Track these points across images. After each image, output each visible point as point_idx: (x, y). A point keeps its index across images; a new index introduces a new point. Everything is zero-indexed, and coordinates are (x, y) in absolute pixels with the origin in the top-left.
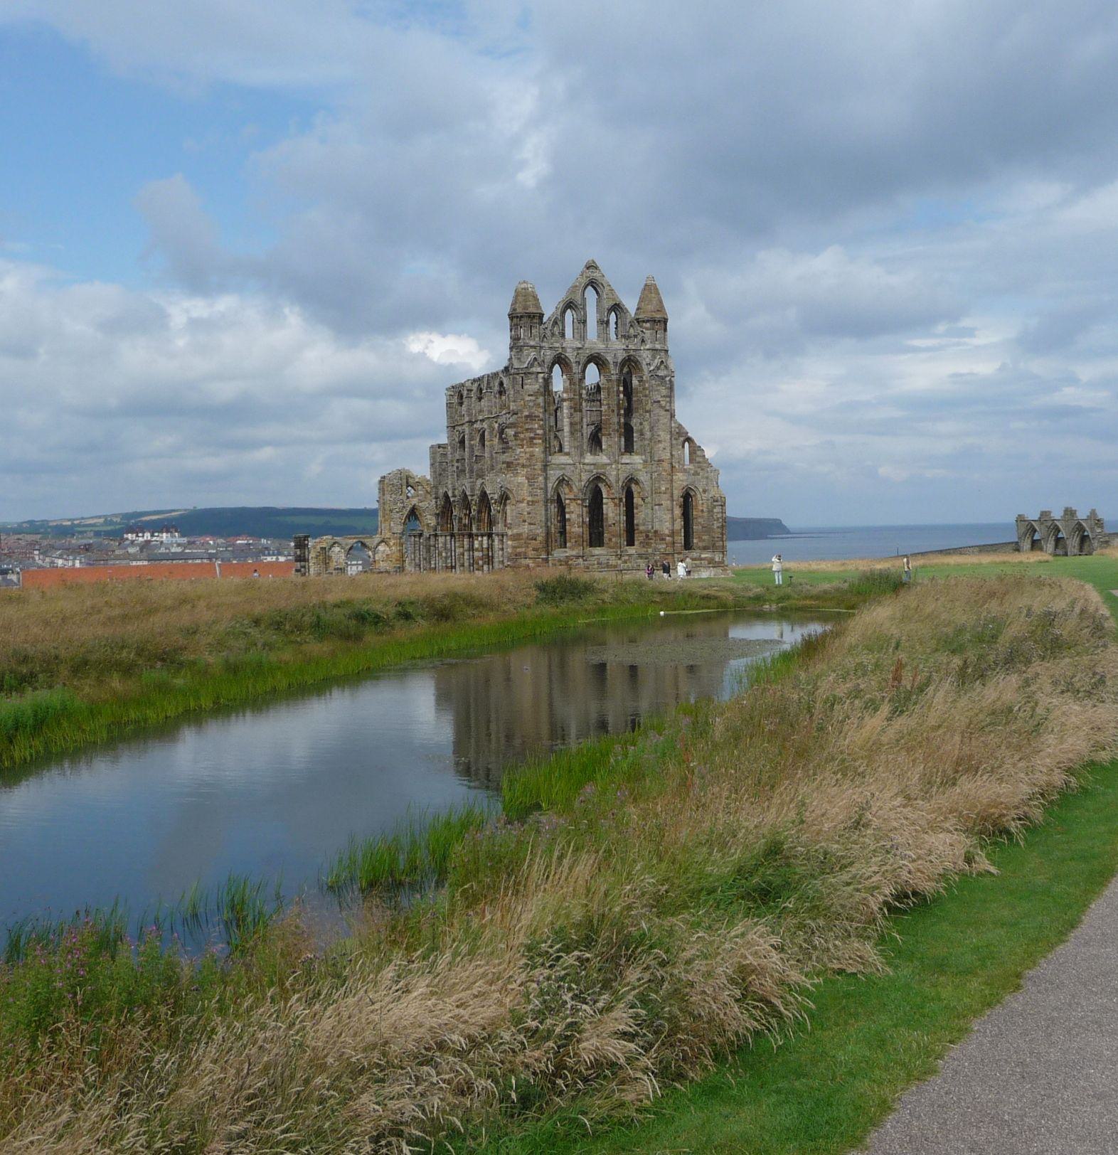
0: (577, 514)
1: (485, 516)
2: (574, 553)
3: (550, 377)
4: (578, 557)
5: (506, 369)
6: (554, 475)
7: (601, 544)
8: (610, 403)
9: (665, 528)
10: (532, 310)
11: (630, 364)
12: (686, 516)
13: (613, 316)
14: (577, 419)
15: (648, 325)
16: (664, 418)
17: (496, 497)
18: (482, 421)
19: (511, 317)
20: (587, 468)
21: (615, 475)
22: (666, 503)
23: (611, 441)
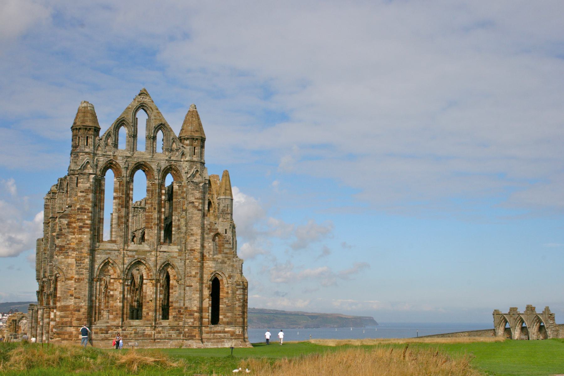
2: (115, 323)
4: (117, 327)
10: (89, 123)
15: (187, 142)
19: (74, 129)
20: (130, 253)
22: (195, 284)
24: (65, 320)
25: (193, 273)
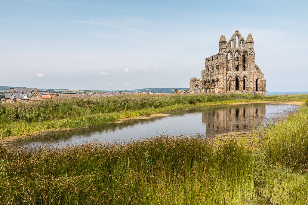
0: (233, 84)
1: (213, 84)
3: (228, 55)
5: (218, 54)
6: (228, 75)
7: (238, 90)
8: (241, 60)
9: (252, 87)
10: (224, 41)
11: (245, 52)
12: (257, 84)
13: (241, 42)
14: (233, 64)
16: (253, 64)
17: (216, 80)
18: (213, 65)
19: (220, 43)
20: (236, 74)
21: (242, 76)
22: (252, 81)
23: (241, 68)
24: (221, 91)
25: (252, 78)
